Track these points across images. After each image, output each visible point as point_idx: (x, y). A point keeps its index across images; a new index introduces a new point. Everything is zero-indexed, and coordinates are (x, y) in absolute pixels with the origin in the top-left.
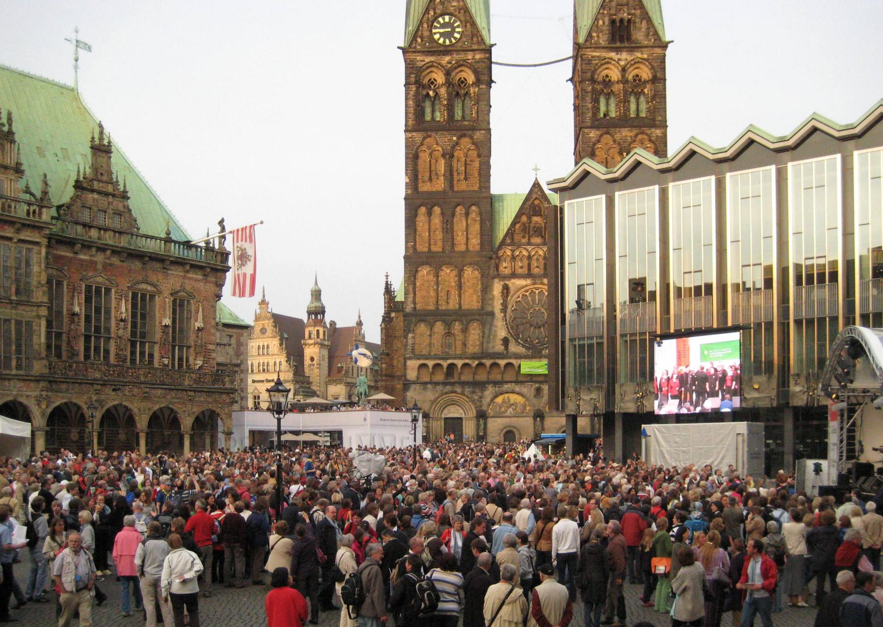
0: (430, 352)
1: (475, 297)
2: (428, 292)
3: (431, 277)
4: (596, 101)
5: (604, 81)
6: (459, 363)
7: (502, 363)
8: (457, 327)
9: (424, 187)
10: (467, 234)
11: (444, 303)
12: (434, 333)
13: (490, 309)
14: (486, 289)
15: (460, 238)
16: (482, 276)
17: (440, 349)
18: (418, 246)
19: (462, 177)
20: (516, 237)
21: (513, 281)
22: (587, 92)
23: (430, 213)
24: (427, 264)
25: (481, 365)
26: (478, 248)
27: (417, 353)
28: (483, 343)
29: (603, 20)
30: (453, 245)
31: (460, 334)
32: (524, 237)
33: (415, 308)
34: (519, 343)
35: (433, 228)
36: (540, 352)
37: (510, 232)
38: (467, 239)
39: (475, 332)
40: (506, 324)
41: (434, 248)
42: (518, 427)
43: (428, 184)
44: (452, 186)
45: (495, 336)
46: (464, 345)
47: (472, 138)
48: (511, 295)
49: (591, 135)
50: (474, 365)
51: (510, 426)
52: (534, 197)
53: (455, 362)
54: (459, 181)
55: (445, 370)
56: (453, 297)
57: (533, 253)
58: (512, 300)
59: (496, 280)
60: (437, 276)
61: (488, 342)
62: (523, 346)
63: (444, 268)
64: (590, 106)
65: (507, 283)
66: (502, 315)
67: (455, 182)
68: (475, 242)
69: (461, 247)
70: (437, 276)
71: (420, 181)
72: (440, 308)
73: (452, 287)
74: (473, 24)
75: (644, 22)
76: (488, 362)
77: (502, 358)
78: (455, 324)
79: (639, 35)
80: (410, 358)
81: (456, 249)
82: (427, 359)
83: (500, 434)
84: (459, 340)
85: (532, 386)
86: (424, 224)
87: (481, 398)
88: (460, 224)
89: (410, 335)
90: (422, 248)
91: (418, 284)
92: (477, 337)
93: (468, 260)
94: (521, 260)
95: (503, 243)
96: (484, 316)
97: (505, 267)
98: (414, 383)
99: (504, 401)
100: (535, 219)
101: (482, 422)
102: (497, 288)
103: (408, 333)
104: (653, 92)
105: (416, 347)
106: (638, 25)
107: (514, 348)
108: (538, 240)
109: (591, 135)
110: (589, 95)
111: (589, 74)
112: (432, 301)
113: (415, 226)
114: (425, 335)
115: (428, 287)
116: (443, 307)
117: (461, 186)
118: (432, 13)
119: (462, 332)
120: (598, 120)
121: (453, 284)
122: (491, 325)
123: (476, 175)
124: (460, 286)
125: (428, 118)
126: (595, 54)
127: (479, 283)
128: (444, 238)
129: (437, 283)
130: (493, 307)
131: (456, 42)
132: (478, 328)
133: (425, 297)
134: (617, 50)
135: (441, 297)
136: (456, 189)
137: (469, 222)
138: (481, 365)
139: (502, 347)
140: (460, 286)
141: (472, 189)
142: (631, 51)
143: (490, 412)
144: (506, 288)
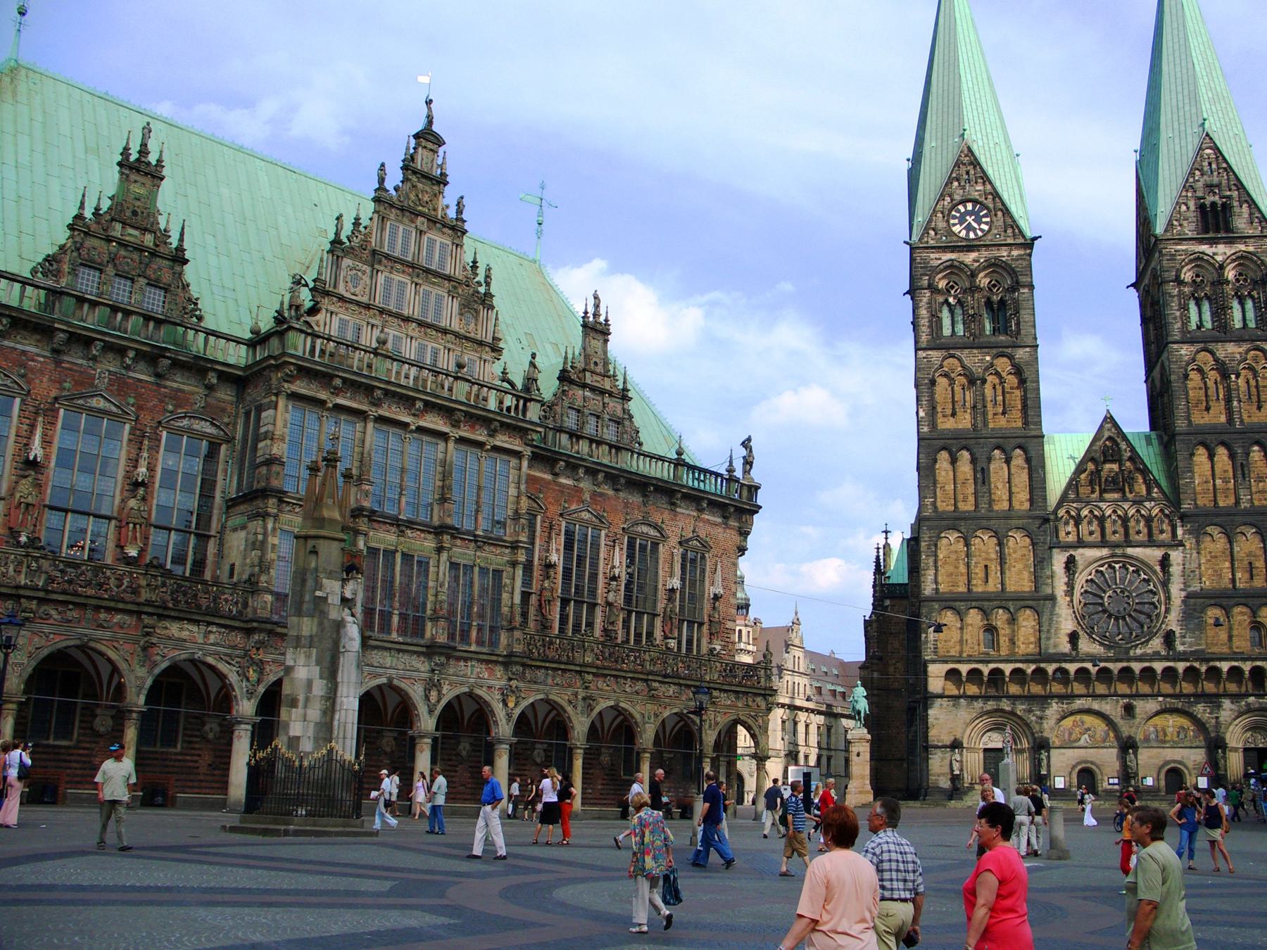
0: (961, 652)
1: (1026, 575)
3: (961, 546)
4: (1185, 308)
5: (1194, 281)
6: (1007, 668)
7: (1072, 668)
9: (946, 424)
10: (1010, 487)
11: (980, 582)
12: (968, 625)
13: (1049, 591)
14: (1041, 564)
15: (1000, 492)
16: (1033, 544)
17: (976, 647)
18: (939, 504)
19: (1000, 410)
20: (1081, 490)
21: (1081, 551)
23: (954, 461)
25: (1040, 672)
26: (1027, 505)
27: (941, 652)
28: (1040, 639)
29: (1186, 204)
30: (991, 502)
32: (1093, 492)
35: (960, 478)
36: (1128, 653)
37: (1073, 484)
39: (1027, 621)
41: (962, 506)
42: (1098, 762)
44: (985, 423)
45: (1057, 629)
46: (1012, 642)
47: (1011, 357)
48: (1079, 571)
49: (1183, 352)
50: (1029, 671)
51: (1086, 762)
52: (1106, 434)
53: (1001, 666)
54: (995, 414)
55: (986, 679)
56: (993, 573)
57: (1108, 512)
58: (1080, 580)
60: (967, 545)
61: (1048, 639)
62: (1101, 644)
64: (1178, 314)
65: (1073, 553)
66: (1068, 599)
67: (990, 416)
68: (1022, 500)
71: (940, 415)
72: (975, 589)
73: (991, 560)
74: (1006, 212)
75: (1245, 205)
76: (1051, 668)
77: (1072, 661)
78: (997, 613)
79: (1241, 221)
80: (934, 661)
81: (996, 508)
82: (959, 662)
83: (1070, 773)
85: (1117, 702)
87: (1041, 718)
90: (945, 506)
91: (941, 556)
93: (1014, 522)
95: (1063, 499)
96: (1039, 601)
97: (1067, 533)
98: (941, 696)
99: (1075, 724)
100: (1108, 466)
101: (1044, 755)
102: (1059, 559)
106: (1237, 210)
107: (1085, 646)
109: (1183, 352)
110: (1176, 299)
111: (1174, 273)
113: (934, 476)
114: (953, 629)
115: (957, 559)
116: (979, 588)
117: (1002, 422)
118: (948, 199)
119: (1009, 624)
120: (1189, 332)
121: (993, 556)
122: (1052, 614)
124: (1002, 560)
125: (947, 331)
126: (1179, 247)
131: (984, 235)
133: (952, 574)
134: (1213, 242)
135: (976, 574)
136: (991, 425)
137: (1013, 471)
138: (1040, 672)
139: (1069, 646)
140: (1002, 560)
141: (1014, 425)
142: (1231, 243)
143: (1054, 741)
144: (1070, 564)
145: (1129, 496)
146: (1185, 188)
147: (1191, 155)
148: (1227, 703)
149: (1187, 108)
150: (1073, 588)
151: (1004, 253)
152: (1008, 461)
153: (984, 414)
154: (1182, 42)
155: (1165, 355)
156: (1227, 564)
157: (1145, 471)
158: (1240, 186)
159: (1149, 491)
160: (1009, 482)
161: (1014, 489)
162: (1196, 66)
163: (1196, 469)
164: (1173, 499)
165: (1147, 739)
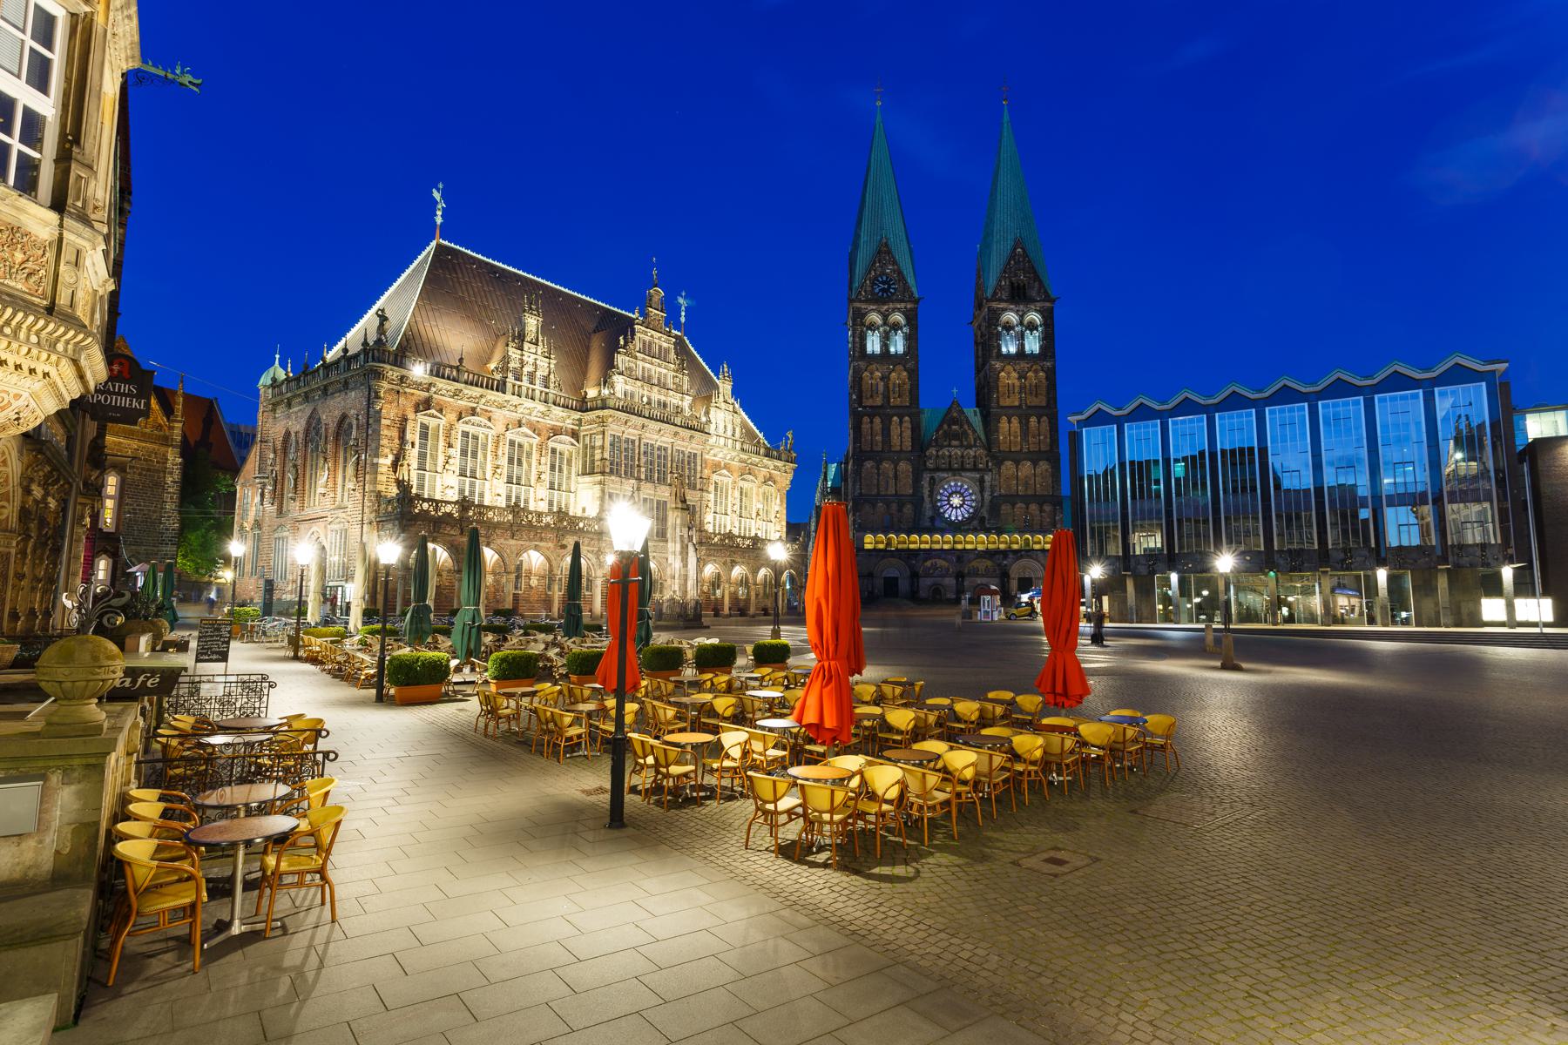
15: (895, 440)
24: (870, 459)
26: (910, 448)
41: (875, 448)
44: (889, 402)
69: (898, 448)
70: (878, 469)
97: (930, 464)
100: (954, 427)
102: (927, 476)
108: (955, 443)
117: (898, 402)
129: (878, 475)
144: (932, 478)
145: (965, 443)
146: (1005, 272)
148: (1011, 556)
151: (903, 305)
152: (901, 422)
153: (889, 398)
155: (987, 367)
156: (1015, 482)
157: (974, 431)
158: (1035, 272)
159: (975, 442)
160: (901, 435)
163: (1001, 430)
164: (989, 444)
165: (969, 573)
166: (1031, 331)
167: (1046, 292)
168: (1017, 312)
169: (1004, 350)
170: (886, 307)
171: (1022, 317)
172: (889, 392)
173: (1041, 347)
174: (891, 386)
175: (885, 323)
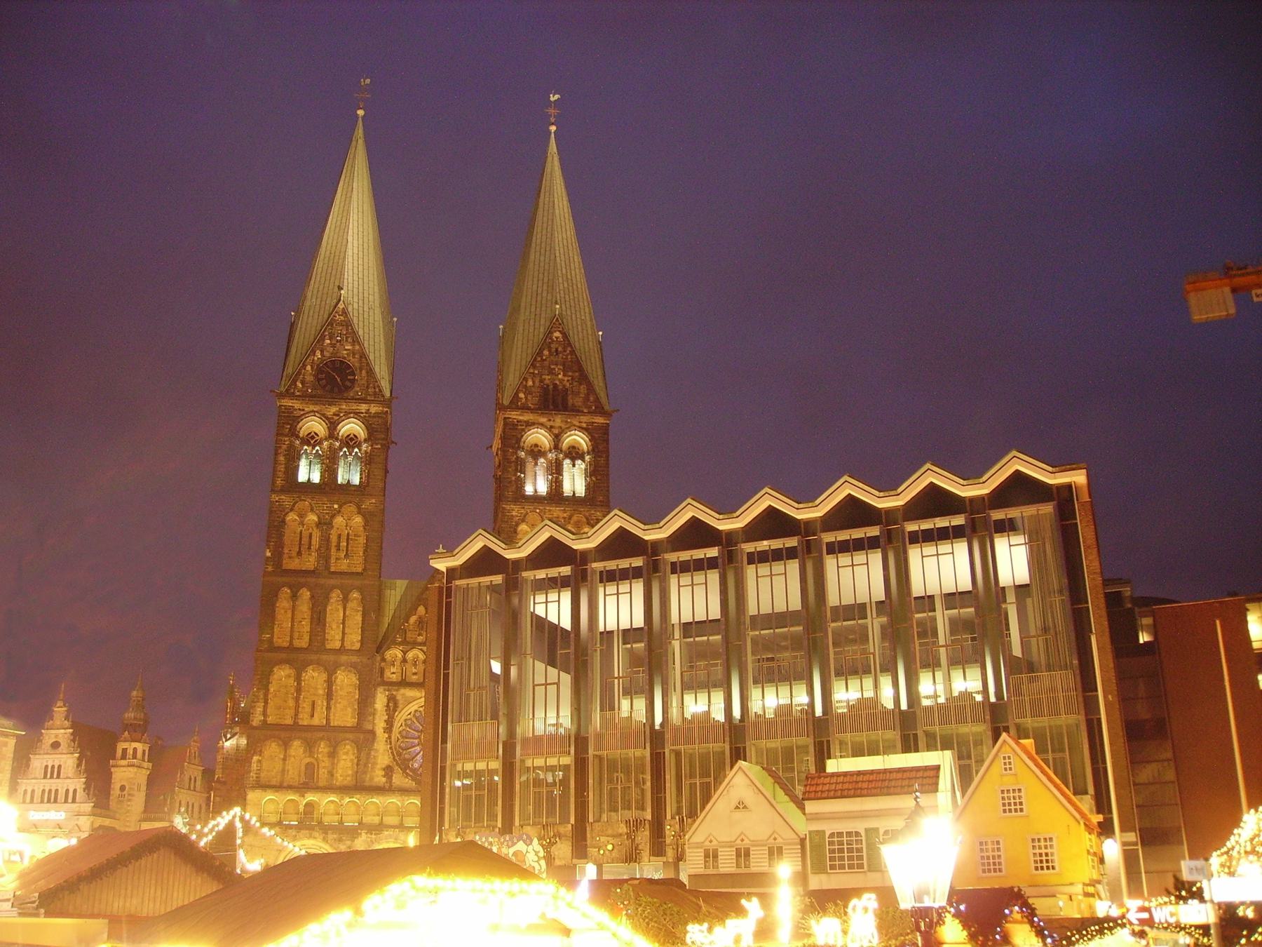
1: (349, 710)
2: (286, 701)
3: (291, 682)
8: (323, 748)
10: (344, 628)
11: (306, 716)
12: (290, 756)
13: (370, 727)
14: (364, 703)
17: (297, 778)
20: (409, 635)
21: (402, 691)
22: (511, 463)
26: (357, 646)
30: (324, 640)
31: (326, 759)
33: (265, 722)
34: (407, 774)
35: (298, 617)
38: (344, 633)
40: (391, 748)
41: (297, 643)
43: (297, 561)
44: (327, 567)
45: (375, 764)
46: (331, 774)
48: (399, 710)
54: (337, 559)
58: (401, 717)
59: (380, 689)
60: (298, 679)
61: (365, 773)
62: (413, 780)
63: (310, 669)
67: (333, 561)
69: (337, 645)
84: (324, 767)
86: (286, 612)
88: (334, 612)
89: (255, 758)
91: (272, 690)
92: (350, 764)
94: (415, 665)
97: (392, 674)
103: (253, 755)
104: (592, 466)
105: (262, 775)
109: (514, 513)
112: (290, 712)
116: (305, 720)
117: (344, 565)
119: (329, 757)
121: (321, 692)
123: (361, 554)
124: (329, 695)
127: (357, 691)
128: (311, 631)
129: (299, 690)
130: (374, 724)
132: (351, 752)
135: (303, 708)
140: (329, 695)
144: (392, 700)
146: (533, 366)
147: (541, 336)
149: (545, 295)
150: (392, 726)
151: (363, 407)
153: (327, 558)
154: (549, 235)
160: (343, 623)
161: (347, 630)
162: (558, 259)
166: (573, 460)
167: (597, 400)
168: (550, 429)
169: (529, 490)
170: (334, 409)
171: (557, 438)
172: (328, 549)
173: (588, 488)
174: (334, 539)
175: (332, 435)
